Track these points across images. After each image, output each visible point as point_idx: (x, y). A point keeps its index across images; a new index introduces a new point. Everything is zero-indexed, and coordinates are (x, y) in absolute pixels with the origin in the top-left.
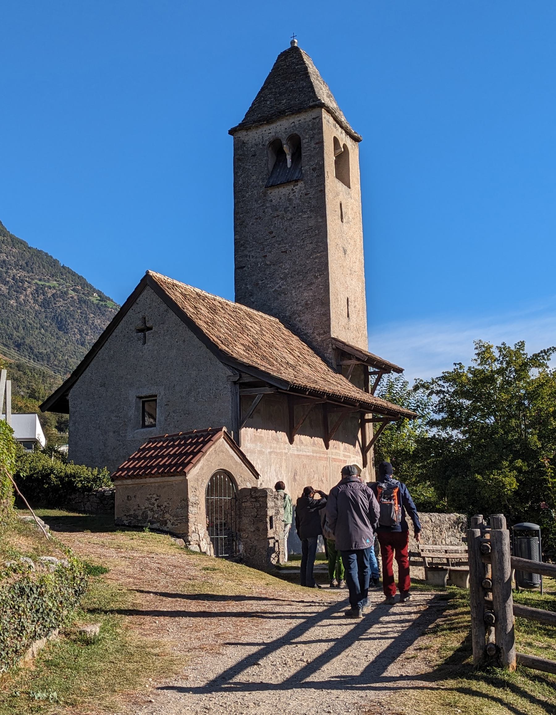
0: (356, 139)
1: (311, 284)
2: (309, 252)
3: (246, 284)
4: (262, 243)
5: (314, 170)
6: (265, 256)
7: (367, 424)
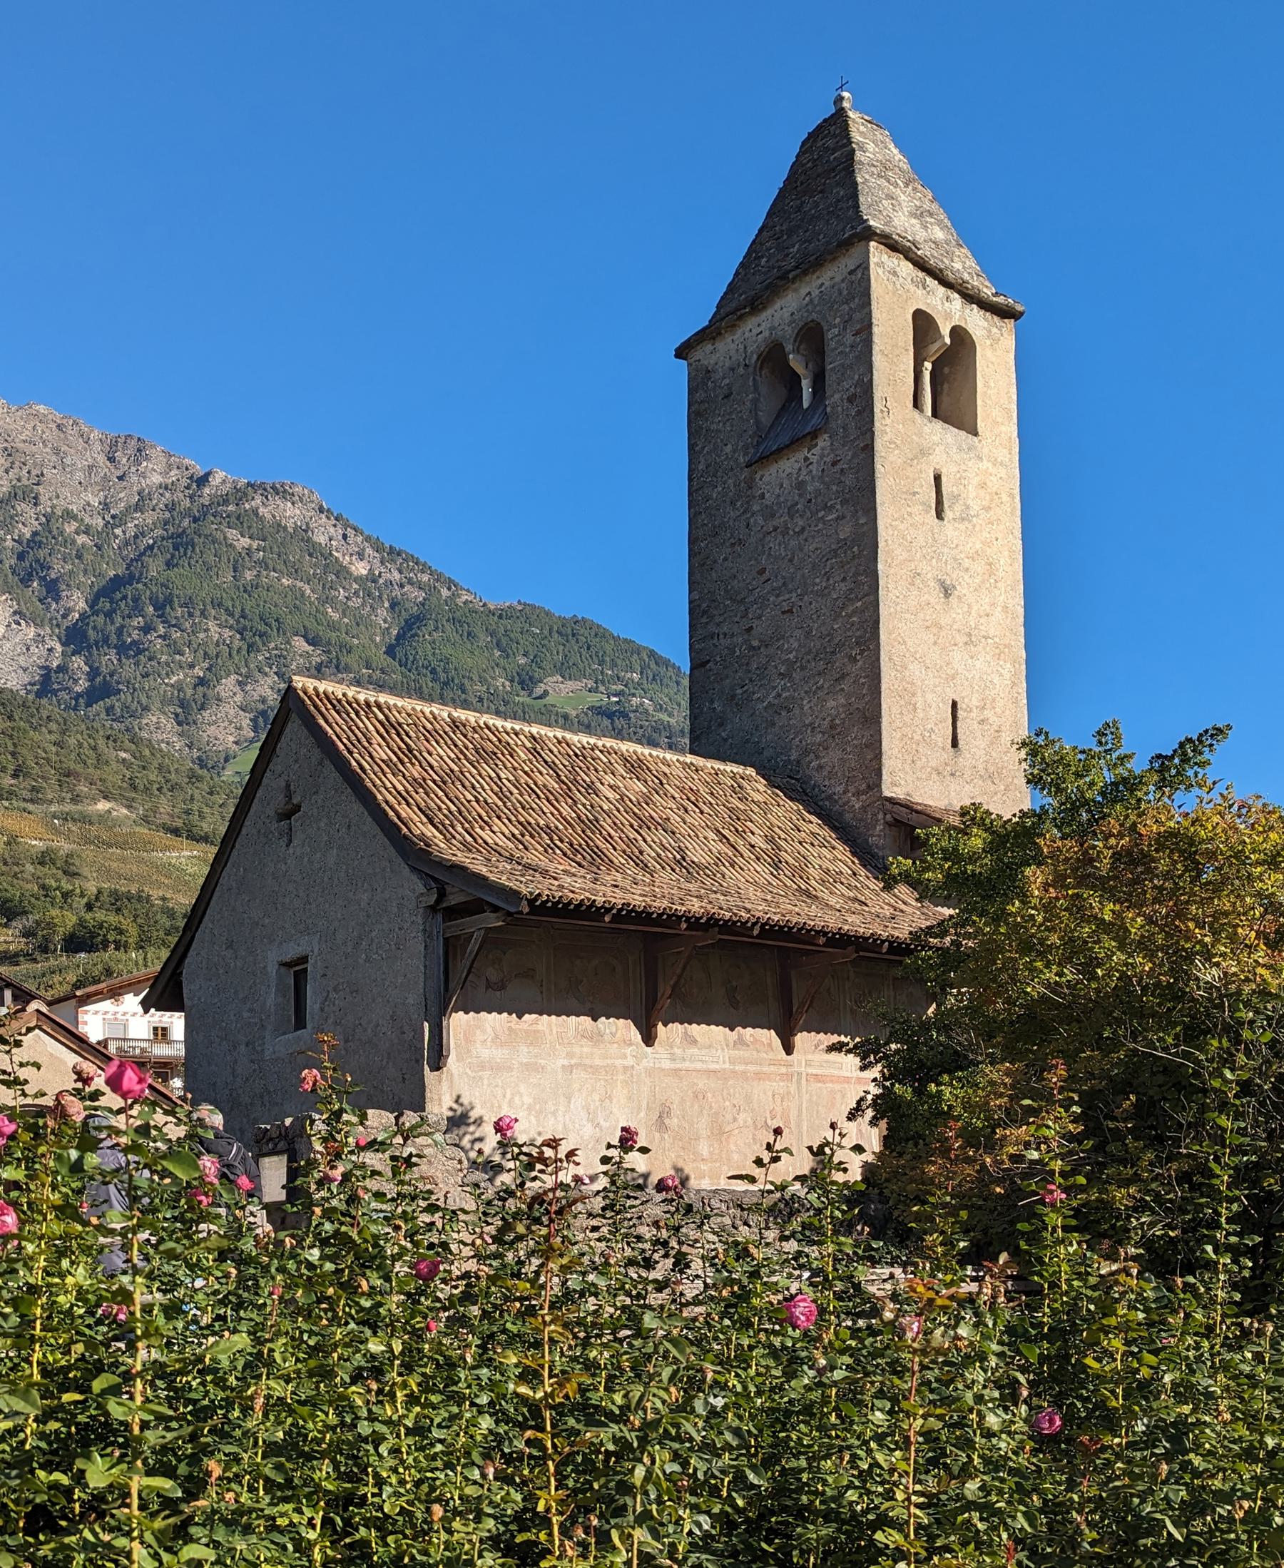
1: (843, 677)
2: (839, 603)
3: (712, 702)
4: (742, 601)
6: (750, 629)
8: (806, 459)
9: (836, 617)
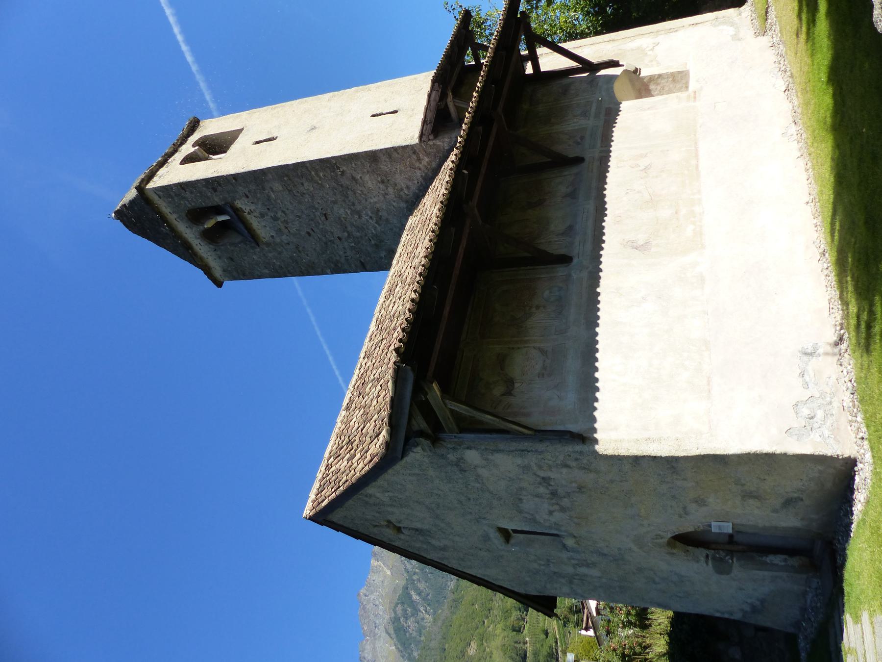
0: (194, 125)
1: (353, 178)
2: (315, 185)
3: (381, 258)
4: (326, 243)
5: (215, 190)
6: (340, 238)
7: (543, 69)
8: (249, 213)
9: (322, 186)
